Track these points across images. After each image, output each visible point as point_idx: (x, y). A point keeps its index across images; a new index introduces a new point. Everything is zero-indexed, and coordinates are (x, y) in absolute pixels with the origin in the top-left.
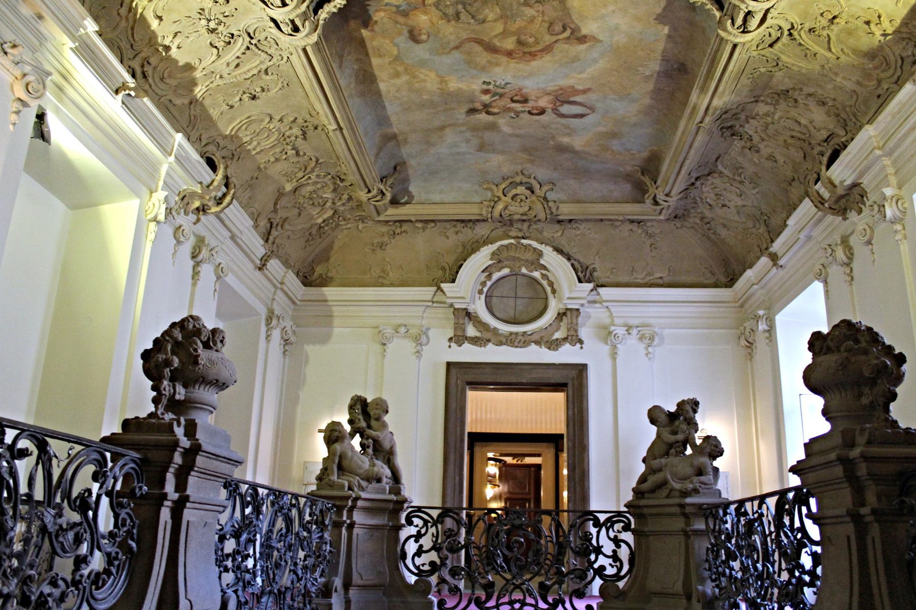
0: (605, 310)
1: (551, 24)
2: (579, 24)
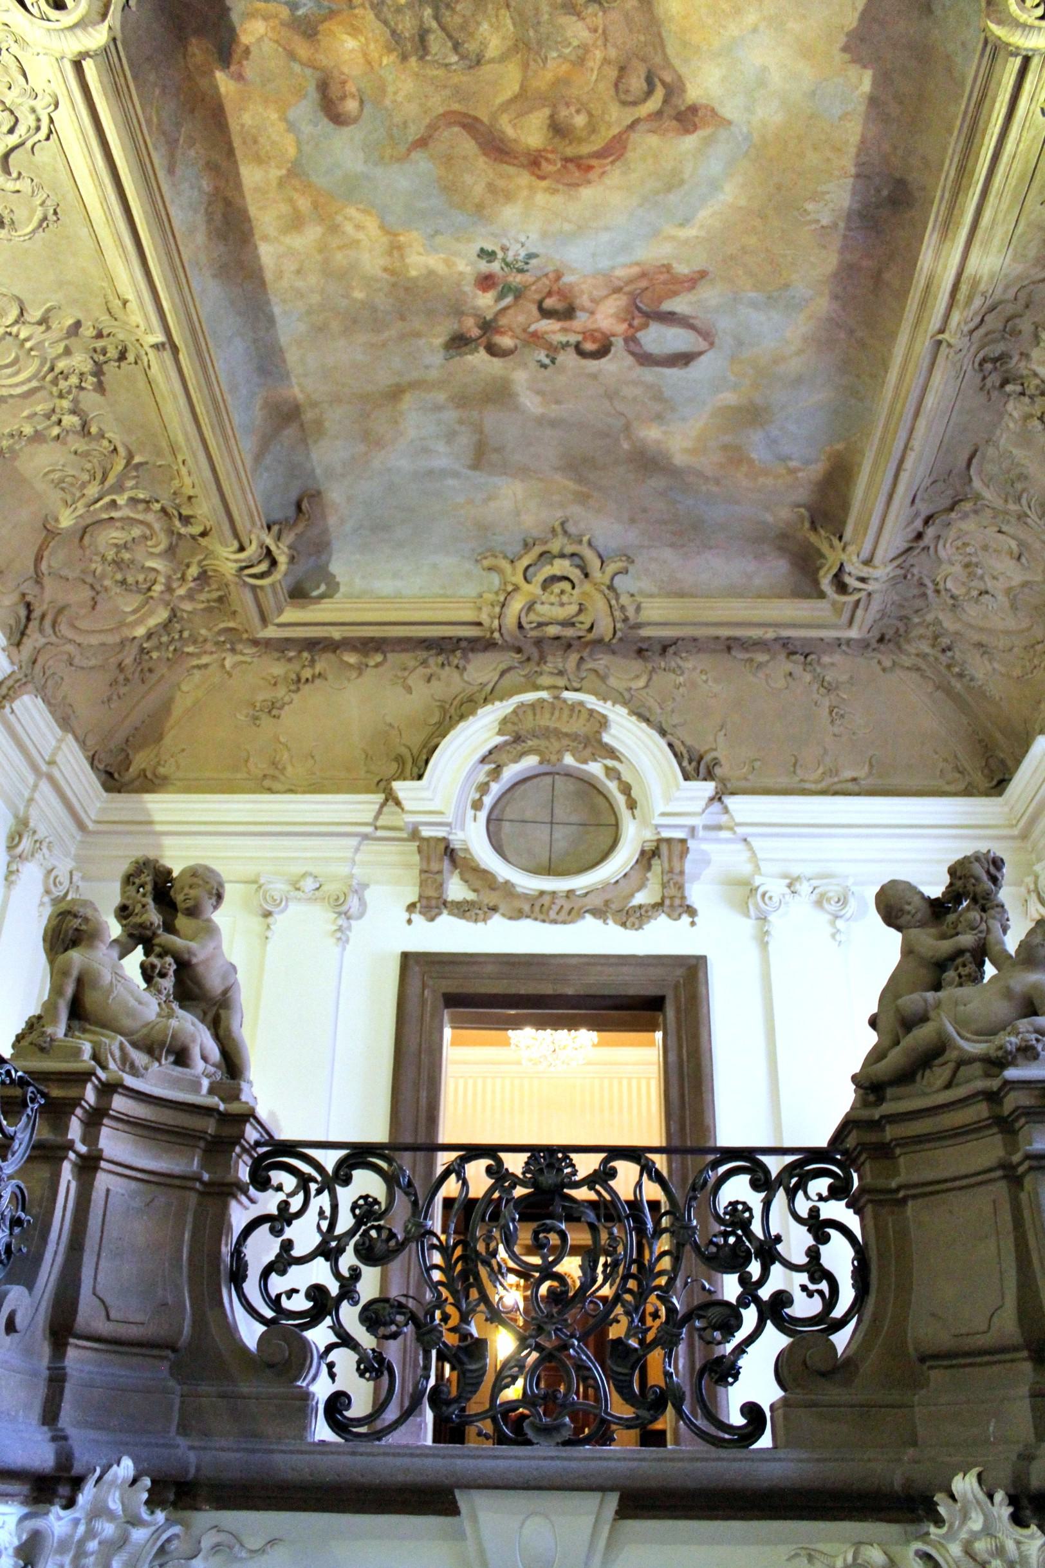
0: (741, 846)
1: (622, 69)
2: (683, 70)
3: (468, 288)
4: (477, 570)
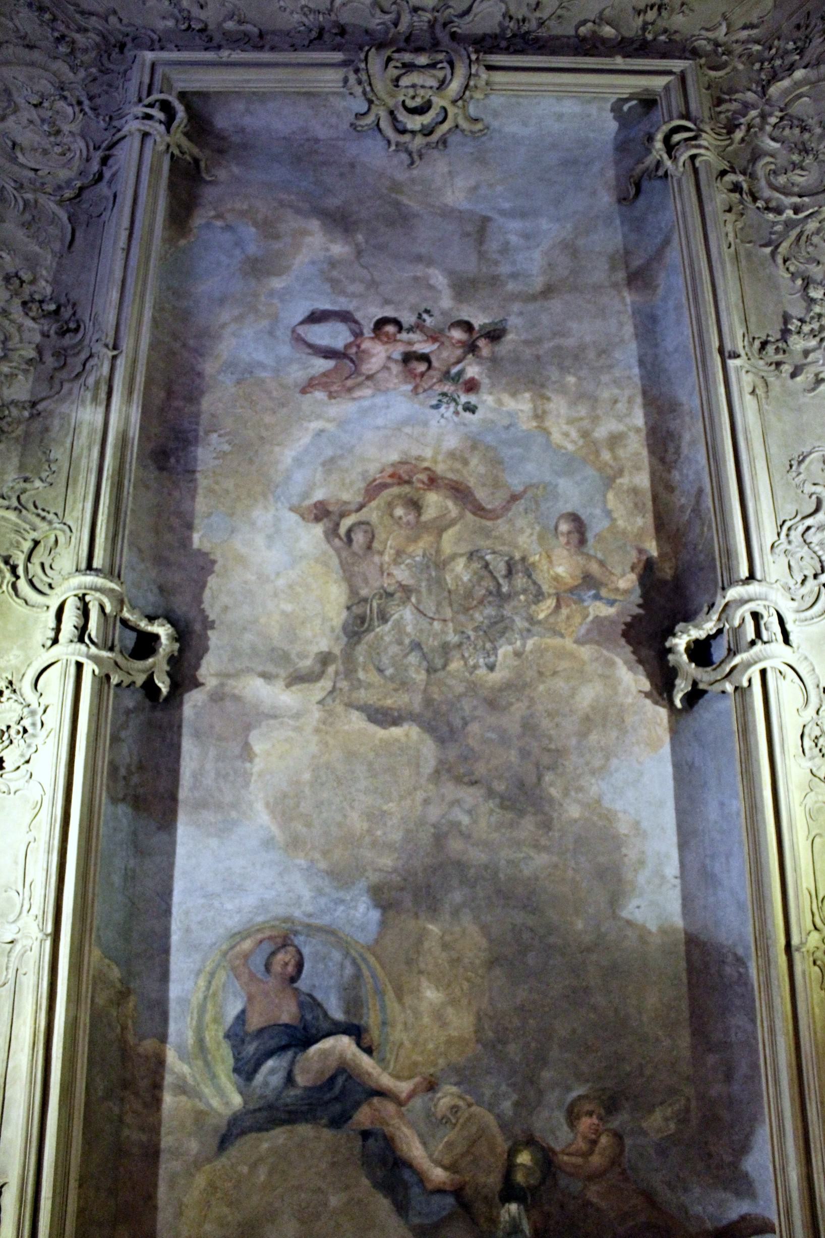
1: (369, 547)
2: (325, 546)
3: (485, 381)
4: (488, 119)
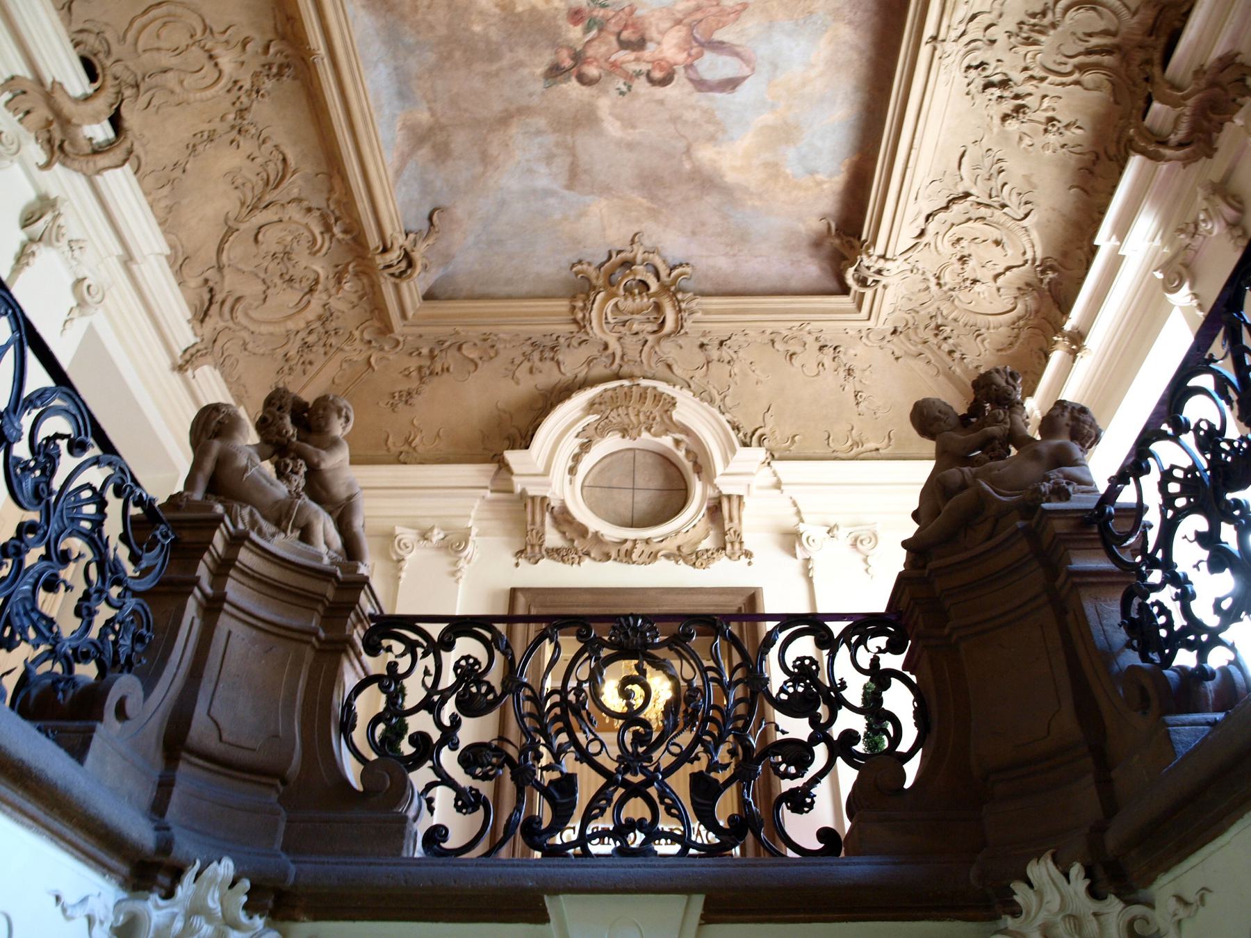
3: (563, 22)
